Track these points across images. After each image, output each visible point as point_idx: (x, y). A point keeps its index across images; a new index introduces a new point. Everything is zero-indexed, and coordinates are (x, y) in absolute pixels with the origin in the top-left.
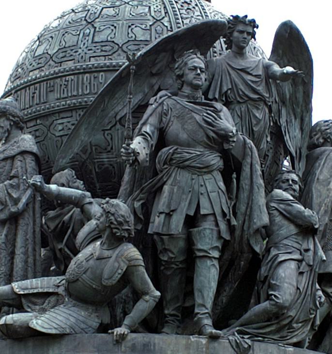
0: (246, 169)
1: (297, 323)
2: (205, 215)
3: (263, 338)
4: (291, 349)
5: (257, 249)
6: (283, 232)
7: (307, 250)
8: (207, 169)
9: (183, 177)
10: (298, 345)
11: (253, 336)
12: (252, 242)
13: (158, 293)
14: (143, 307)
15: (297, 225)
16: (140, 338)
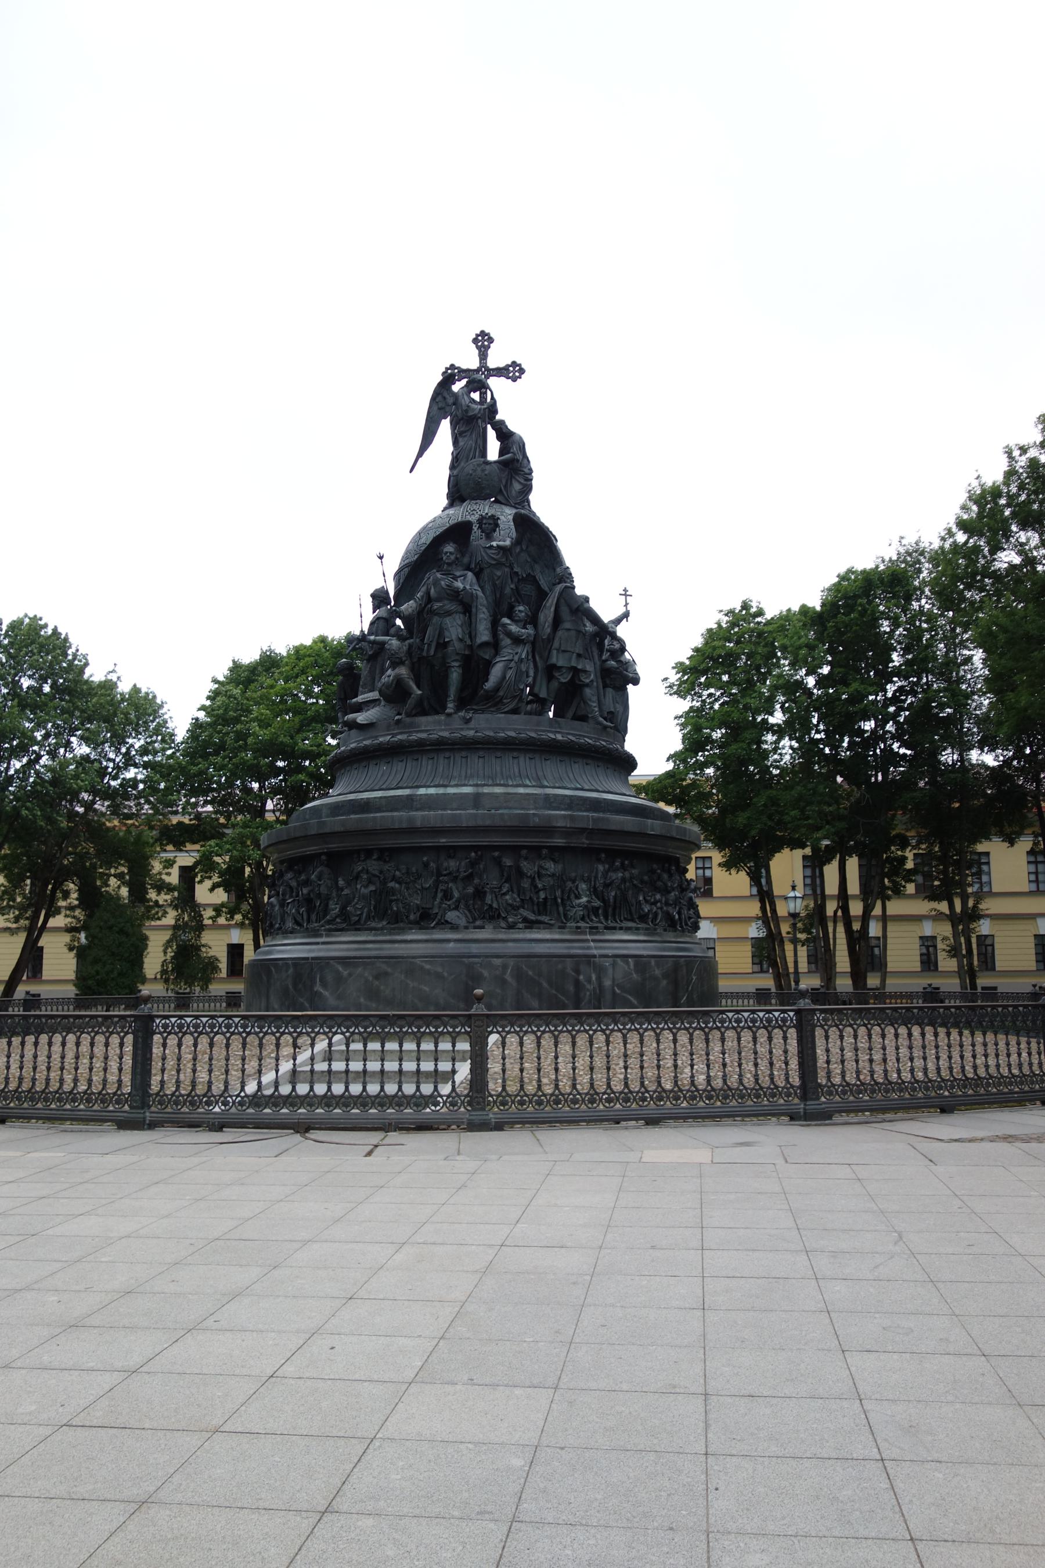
0: (474, 610)
1: (506, 698)
2: (449, 642)
3: (483, 711)
4: (503, 715)
5: (487, 657)
6: (503, 643)
7: (517, 653)
8: (449, 613)
9: (436, 619)
10: (515, 711)
11: (476, 711)
12: (481, 654)
13: (420, 692)
14: (411, 702)
15: (511, 639)
16: (408, 720)
